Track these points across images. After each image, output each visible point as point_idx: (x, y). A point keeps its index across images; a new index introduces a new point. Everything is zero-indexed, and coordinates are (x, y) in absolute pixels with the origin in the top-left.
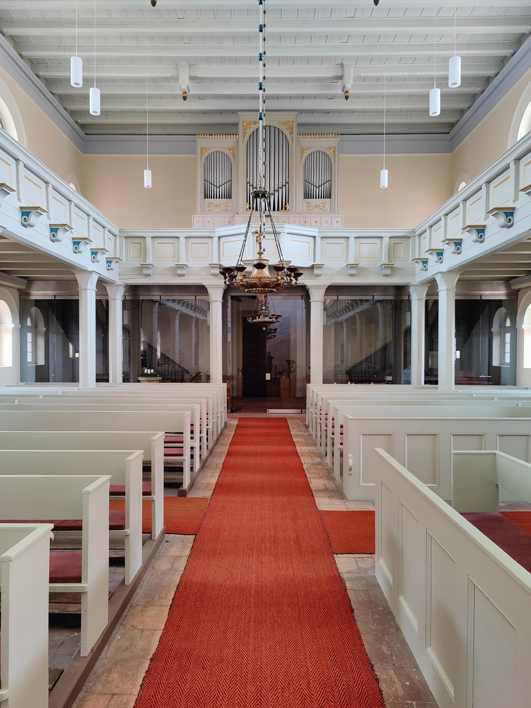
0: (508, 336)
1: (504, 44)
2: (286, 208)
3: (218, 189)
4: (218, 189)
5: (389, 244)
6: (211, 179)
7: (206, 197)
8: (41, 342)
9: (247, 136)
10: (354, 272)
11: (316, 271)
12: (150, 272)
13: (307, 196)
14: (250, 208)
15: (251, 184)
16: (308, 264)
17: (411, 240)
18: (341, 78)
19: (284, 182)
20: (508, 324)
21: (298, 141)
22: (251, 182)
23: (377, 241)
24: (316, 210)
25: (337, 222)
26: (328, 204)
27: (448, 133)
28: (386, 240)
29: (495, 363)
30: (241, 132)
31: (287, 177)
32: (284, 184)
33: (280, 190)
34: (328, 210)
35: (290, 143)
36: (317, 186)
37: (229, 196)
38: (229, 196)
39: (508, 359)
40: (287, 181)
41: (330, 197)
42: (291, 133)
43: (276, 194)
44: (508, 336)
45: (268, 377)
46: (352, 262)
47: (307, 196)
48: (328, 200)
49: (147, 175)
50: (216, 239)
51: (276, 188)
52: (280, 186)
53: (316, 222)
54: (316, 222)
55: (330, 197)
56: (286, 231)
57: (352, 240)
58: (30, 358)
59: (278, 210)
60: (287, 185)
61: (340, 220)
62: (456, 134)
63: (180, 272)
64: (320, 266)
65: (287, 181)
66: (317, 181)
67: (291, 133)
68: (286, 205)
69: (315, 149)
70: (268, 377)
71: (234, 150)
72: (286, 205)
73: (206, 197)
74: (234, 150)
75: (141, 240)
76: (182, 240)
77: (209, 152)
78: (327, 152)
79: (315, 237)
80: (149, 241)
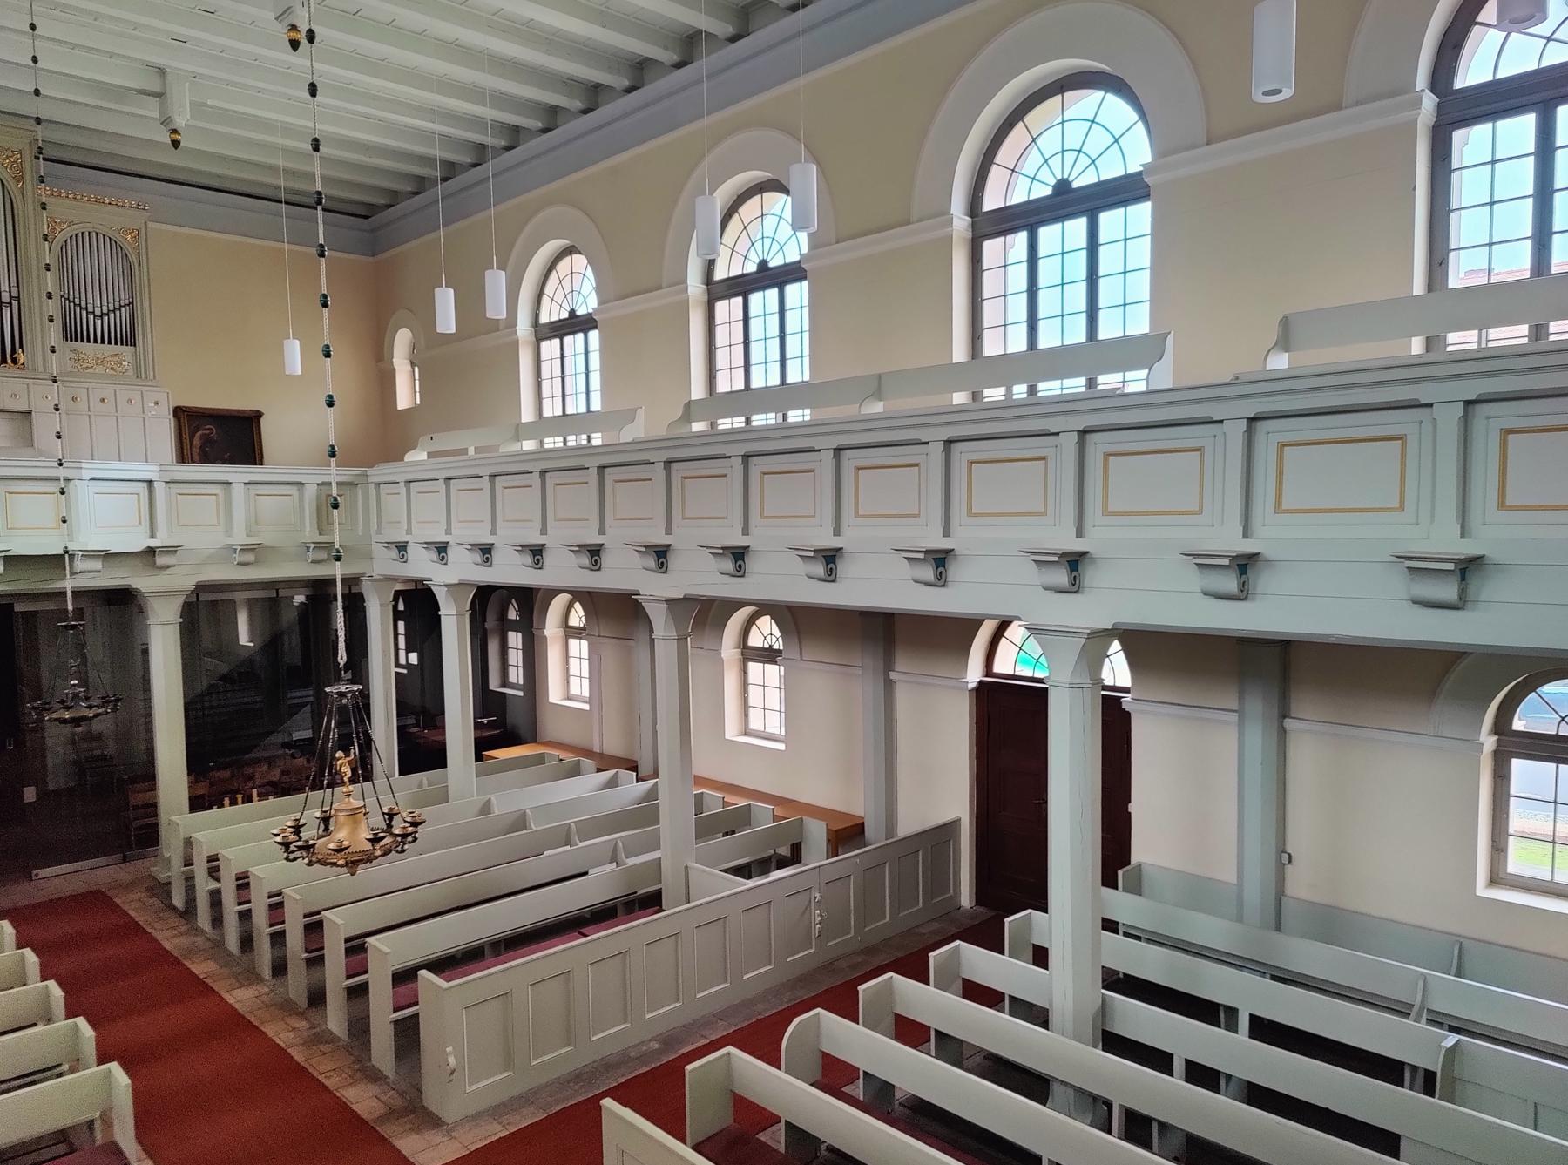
0: (515, 639)
2: (15, 361)
5: (318, 497)
10: (250, 557)
11: (161, 560)
16: (140, 542)
17: (359, 490)
20: (512, 614)
23: (293, 490)
24: (100, 370)
26: (129, 358)
28: (311, 491)
29: (494, 684)
31: (13, 282)
34: (131, 372)
35: (17, 198)
36: (98, 312)
39: (516, 675)
40: (15, 294)
41: (133, 344)
44: (515, 639)
45: (30, 794)
46: (240, 537)
48: (127, 350)
55: (133, 344)
57: (238, 490)
60: (15, 303)
64: (171, 550)
65: (15, 294)
66: (94, 300)
67: (19, 179)
68: (13, 351)
69: (86, 228)
70: (30, 794)
72: (13, 351)
78: (119, 238)
79: (150, 482)
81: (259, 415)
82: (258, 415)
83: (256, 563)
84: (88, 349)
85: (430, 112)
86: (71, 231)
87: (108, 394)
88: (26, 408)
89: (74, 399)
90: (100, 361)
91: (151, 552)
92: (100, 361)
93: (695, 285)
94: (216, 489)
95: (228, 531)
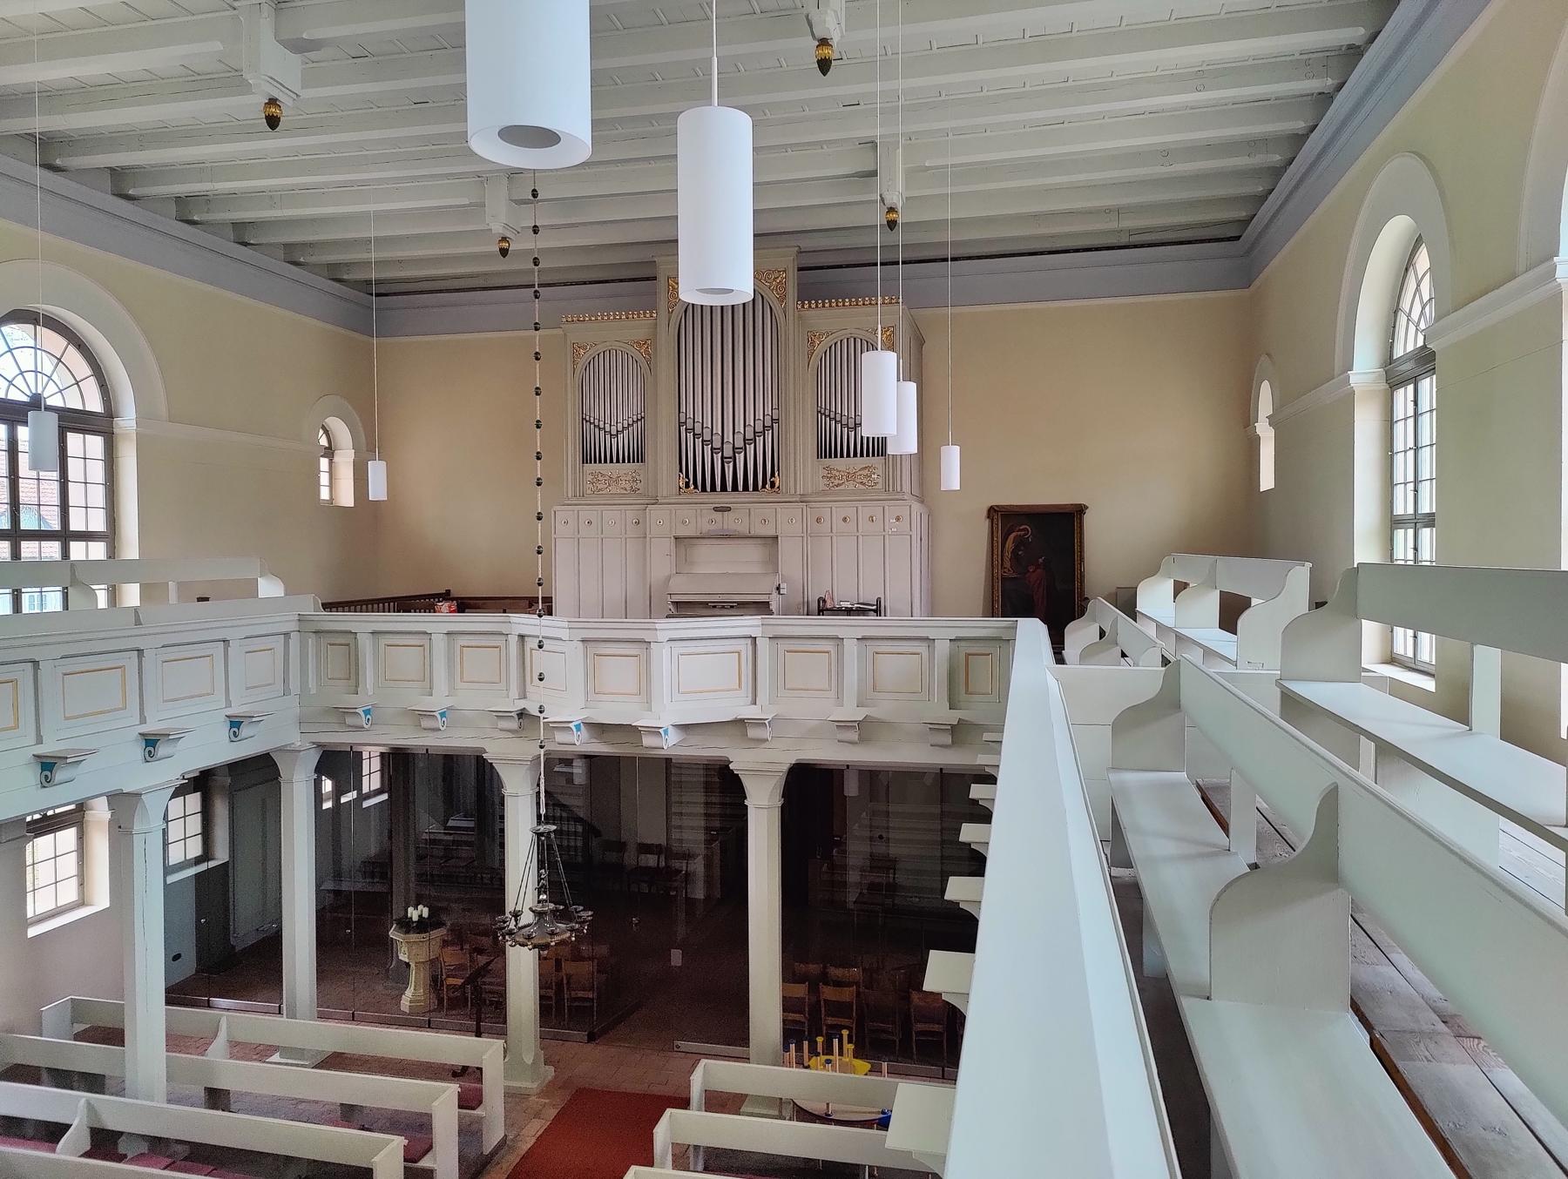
1: (1307, 63)
3: (614, 441)
4: (614, 441)
5: (952, 658)
6: (597, 414)
7: (586, 460)
10: (854, 736)
11: (753, 733)
13: (827, 450)
14: (687, 485)
15: (690, 425)
18: (874, 174)
19: (768, 419)
21: (800, 317)
22: (690, 422)
23: (922, 648)
24: (850, 486)
25: (898, 519)
27: (1238, 238)
28: (942, 648)
32: (768, 423)
33: (760, 440)
34: (879, 486)
37: (638, 456)
38: (638, 456)
42: (782, 299)
43: (750, 449)
47: (827, 450)
50: (513, 640)
51: (750, 435)
52: (759, 428)
53: (845, 520)
54: (845, 520)
57: (851, 648)
59: (756, 488)
61: (905, 512)
62: (1261, 235)
63: (426, 723)
64: (760, 723)
67: (782, 299)
68: (773, 475)
71: (648, 345)
72: (773, 475)
73: (586, 460)
74: (648, 345)
76: (439, 643)
77: (592, 352)
80: (365, 643)
81: (1079, 511)
82: (1079, 511)
84: (839, 464)
85: (1203, 76)
86: (827, 342)
87: (850, 512)
88: (772, 533)
89: (818, 520)
90: (850, 476)
91: (740, 723)
92: (850, 476)
93: (127, 420)
94: (829, 646)
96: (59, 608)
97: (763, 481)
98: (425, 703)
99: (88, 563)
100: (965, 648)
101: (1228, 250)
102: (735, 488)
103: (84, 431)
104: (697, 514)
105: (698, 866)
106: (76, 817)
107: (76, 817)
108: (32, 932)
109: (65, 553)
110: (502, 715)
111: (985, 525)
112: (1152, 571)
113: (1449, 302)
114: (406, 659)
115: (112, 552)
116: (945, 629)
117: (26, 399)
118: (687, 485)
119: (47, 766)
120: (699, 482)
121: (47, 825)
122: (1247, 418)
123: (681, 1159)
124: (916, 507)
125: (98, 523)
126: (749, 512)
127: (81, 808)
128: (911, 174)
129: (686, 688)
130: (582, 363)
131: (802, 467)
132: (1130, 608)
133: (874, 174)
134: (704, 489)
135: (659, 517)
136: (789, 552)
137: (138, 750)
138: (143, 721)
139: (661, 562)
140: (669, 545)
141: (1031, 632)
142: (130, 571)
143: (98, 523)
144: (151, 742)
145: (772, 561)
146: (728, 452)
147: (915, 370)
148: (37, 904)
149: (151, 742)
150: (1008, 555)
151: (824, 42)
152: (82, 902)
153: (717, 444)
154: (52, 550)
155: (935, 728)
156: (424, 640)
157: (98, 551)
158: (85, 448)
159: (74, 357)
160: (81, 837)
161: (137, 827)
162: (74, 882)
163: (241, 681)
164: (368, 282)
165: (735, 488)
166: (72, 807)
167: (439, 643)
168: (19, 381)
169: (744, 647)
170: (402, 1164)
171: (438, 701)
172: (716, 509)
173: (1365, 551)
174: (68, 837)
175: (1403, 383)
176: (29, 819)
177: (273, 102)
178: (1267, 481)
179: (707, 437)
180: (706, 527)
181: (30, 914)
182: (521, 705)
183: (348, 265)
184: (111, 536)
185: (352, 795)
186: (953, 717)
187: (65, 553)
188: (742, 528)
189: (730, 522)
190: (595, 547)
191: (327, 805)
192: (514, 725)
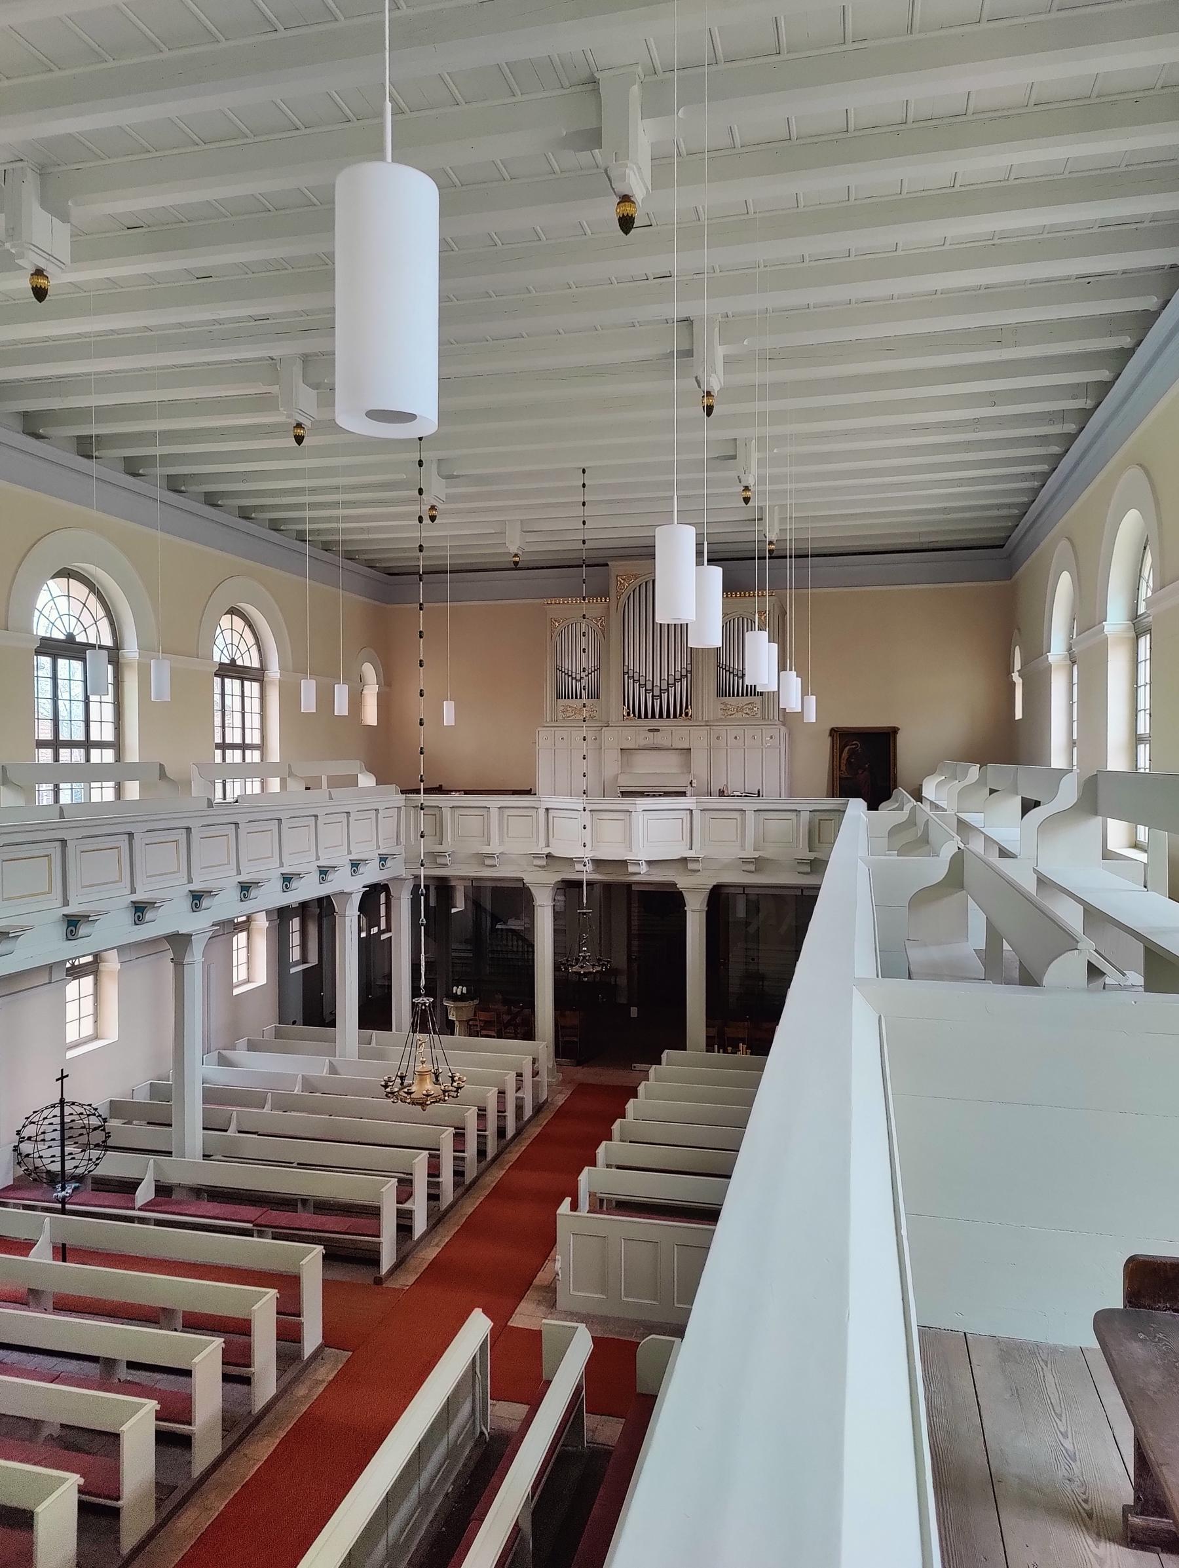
2: (687, 714)
6: (568, 665)
8: (313, 930)
9: (624, 598)
10: (752, 867)
11: (691, 866)
12: (448, 860)
13: (723, 691)
14: (628, 714)
23: (792, 816)
24: (739, 715)
26: (759, 705)
28: (805, 816)
30: (613, 593)
33: (678, 685)
34: (759, 716)
46: (750, 853)
47: (723, 691)
49: (449, 708)
50: (542, 812)
56: (640, 808)
57: (750, 816)
58: (295, 954)
59: (675, 717)
61: (775, 732)
63: (488, 862)
64: (696, 860)
75: (436, 811)
76: (494, 813)
80: (447, 813)
81: (894, 731)
82: (894, 731)
83: (757, 871)
91: (684, 860)
94: (736, 815)
95: (743, 847)
96: (51, 802)
97: (680, 712)
98: (487, 850)
99: (101, 765)
100: (818, 816)
101: (987, 567)
102: (661, 716)
103: (70, 658)
104: (635, 734)
105: (622, 981)
106: (93, 968)
107: (93, 968)
108: (236, 992)
109: (56, 758)
110: (537, 856)
111: (827, 742)
112: (931, 772)
113: (1161, 584)
114: (472, 823)
115: (118, 758)
116: (807, 805)
117: (62, 637)
118: (628, 714)
119: (73, 924)
120: (637, 713)
121: (76, 972)
122: (1009, 670)
123: (600, 1204)
124: (783, 730)
125: (109, 736)
126: (673, 733)
127: (97, 958)
128: (761, 463)
129: (652, 839)
130: (557, 631)
131: (707, 703)
132: (919, 798)
133: (734, 457)
134: (640, 717)
135: (611, 737)
136: (699, 760)
137: (187, 903)
138: (190, 881)
139: (611, 765)
140: (616, 754)
141: (856, 807)
142: (133, 772)
143: (109, 736)
144: (197, 897)
145: (687, 766)
146: (657, 692)
147: (779, 636)
148: (71, 1035)
149: (197, 897)
150: (844, 762)
151: (746, 488)
152: (96, 1037)
153: (649, 687)
154: (78, 755)
155: (801, 862)
156: (484, 812)
157: (108, 756)
158: (252, 688)
159: (93, 600)
160: (96, 984)
161: (186, 961)
162: (91, 1019)
163: (358, 841)
164: (303, 532)
165: (661, 716)
166: (90, 959)
167: (494, 813)
168: (58, 623)
169: (685, 815)
170: (426, 1179)
171: (494, 848)
172: (650, 730)
173: (1116, 762)
174: (88, 981)
175: (1144, 633)
176: (68, 965)
177: (433, 508)
178: (1019, 715)
179: (642, 682)
180: (643, 743)
181: (235, 980)
182: (546, 851)
183: (380, 560)
184: (117, 745)
185: (375, 930)
186: (812, 856)
187: (56, 758)
188: (666, 743)
189: (660, 739)
190: (564, 757)
191: (363, 935)
192: (543, 862)
